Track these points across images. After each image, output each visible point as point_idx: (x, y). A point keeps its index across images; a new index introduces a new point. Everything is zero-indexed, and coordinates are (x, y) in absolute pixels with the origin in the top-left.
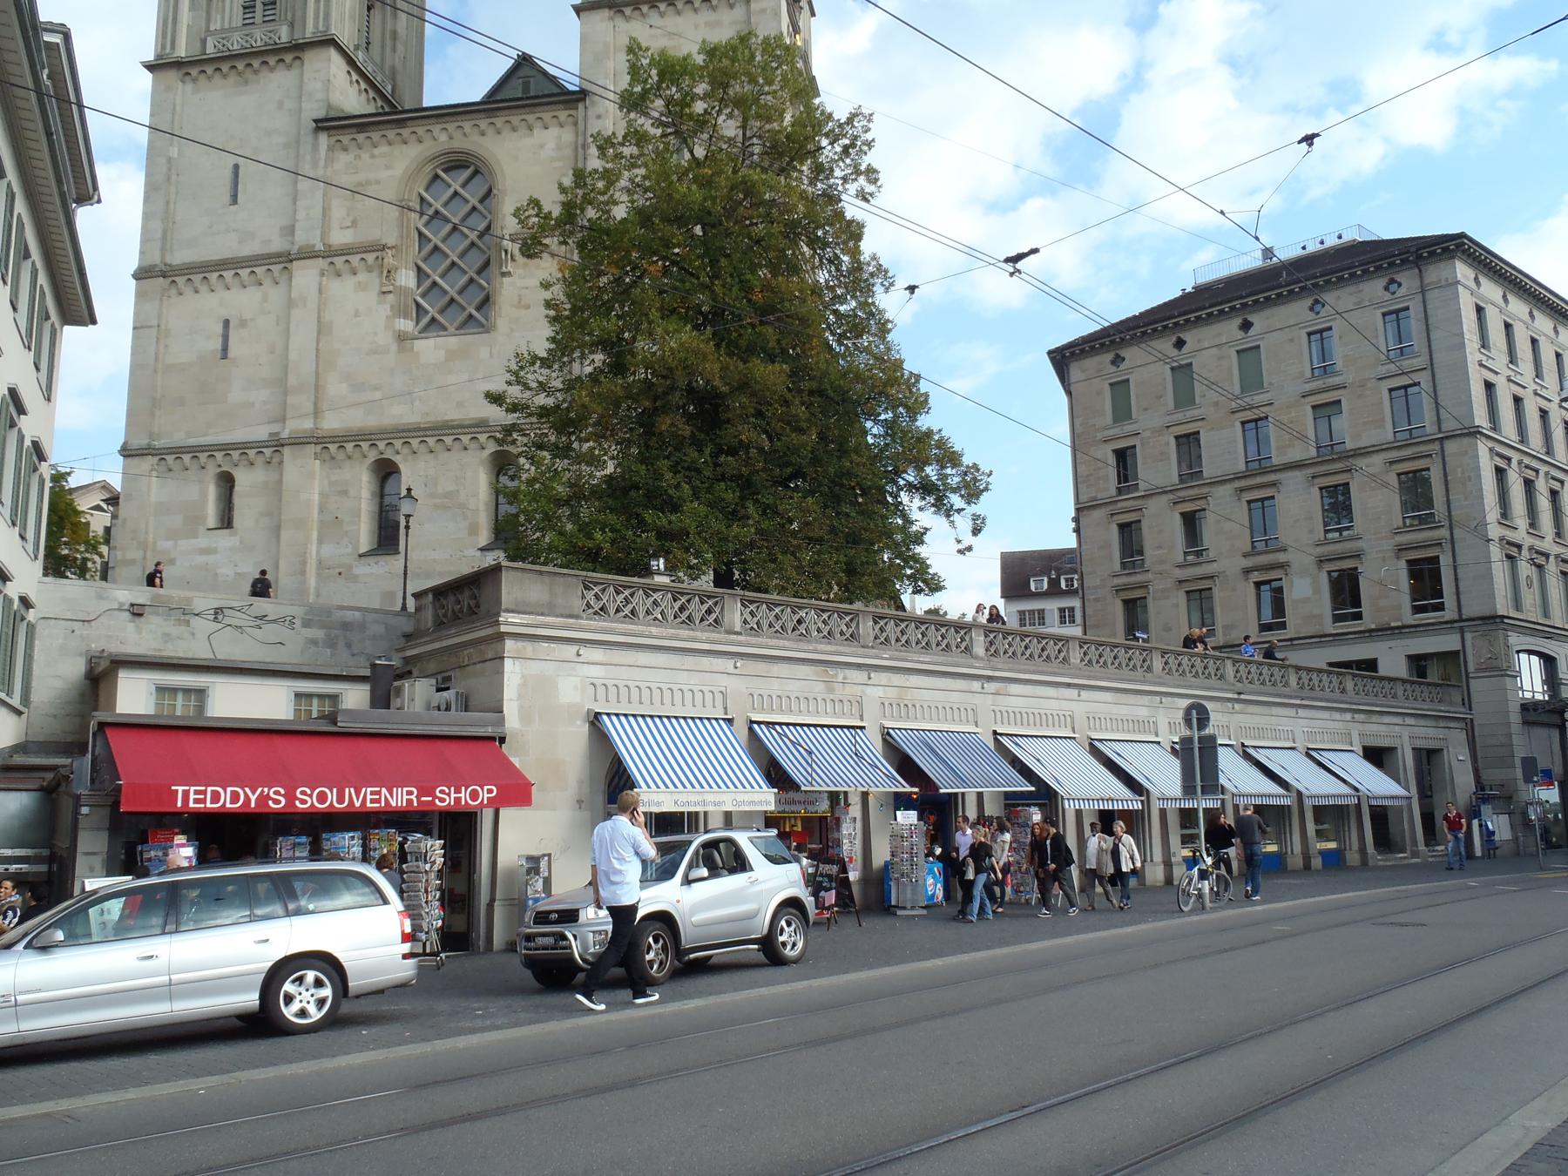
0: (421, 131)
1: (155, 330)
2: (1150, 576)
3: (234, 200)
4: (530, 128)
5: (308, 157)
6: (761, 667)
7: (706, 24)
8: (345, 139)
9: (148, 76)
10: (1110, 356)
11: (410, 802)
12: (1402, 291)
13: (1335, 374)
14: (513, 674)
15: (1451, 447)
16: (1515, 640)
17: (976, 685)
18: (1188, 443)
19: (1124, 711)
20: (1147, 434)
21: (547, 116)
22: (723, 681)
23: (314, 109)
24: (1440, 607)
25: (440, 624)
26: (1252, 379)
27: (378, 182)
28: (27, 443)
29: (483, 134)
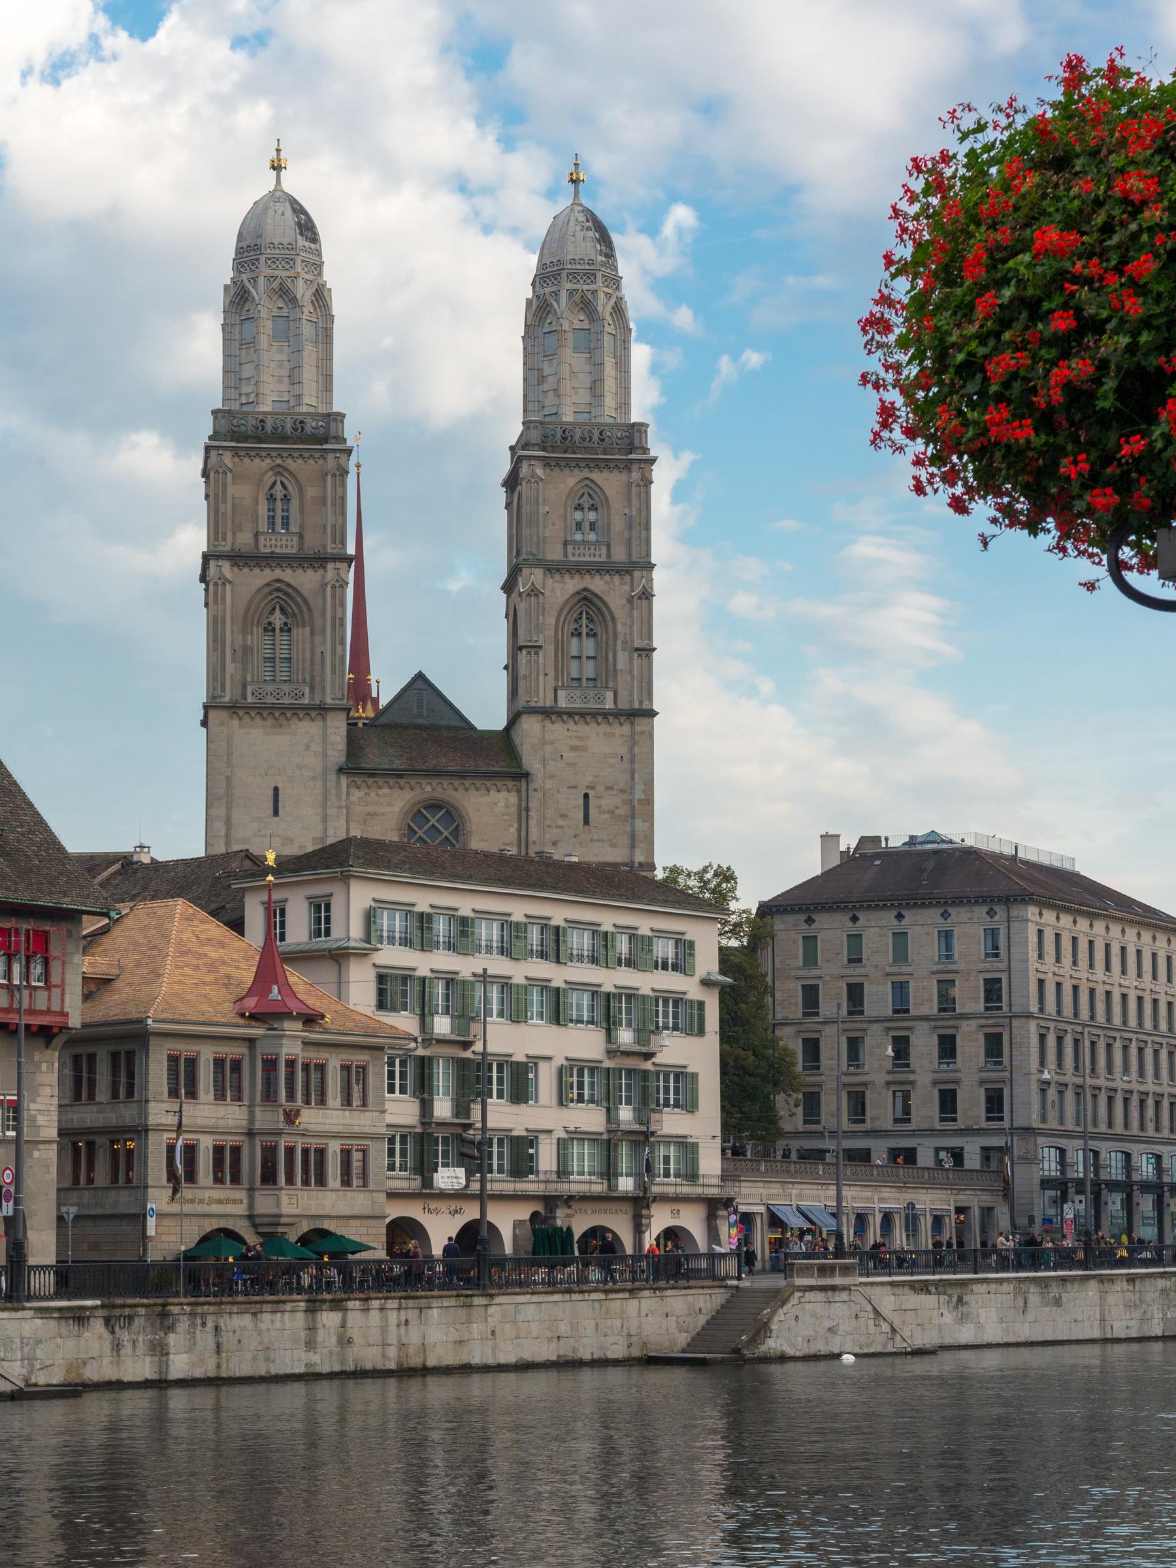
0: (413, 783)
2: (823, 1078)
3: (276, 813)
4: (488, 790)
5: (334, 791)
7: (605, 734)
8: (359, 781)
10: (804, 917)
12: (997, 918)
13: (954, 963)
15: (1016, 1023)
16: (1041, 1140)
18: (855, 993)
19: (864, 1194)
20: (828, 978)
21: (500, 784)
24: (1001, 1119)
26: (901, 953)
27: (383, 814)
29: (456, 790)
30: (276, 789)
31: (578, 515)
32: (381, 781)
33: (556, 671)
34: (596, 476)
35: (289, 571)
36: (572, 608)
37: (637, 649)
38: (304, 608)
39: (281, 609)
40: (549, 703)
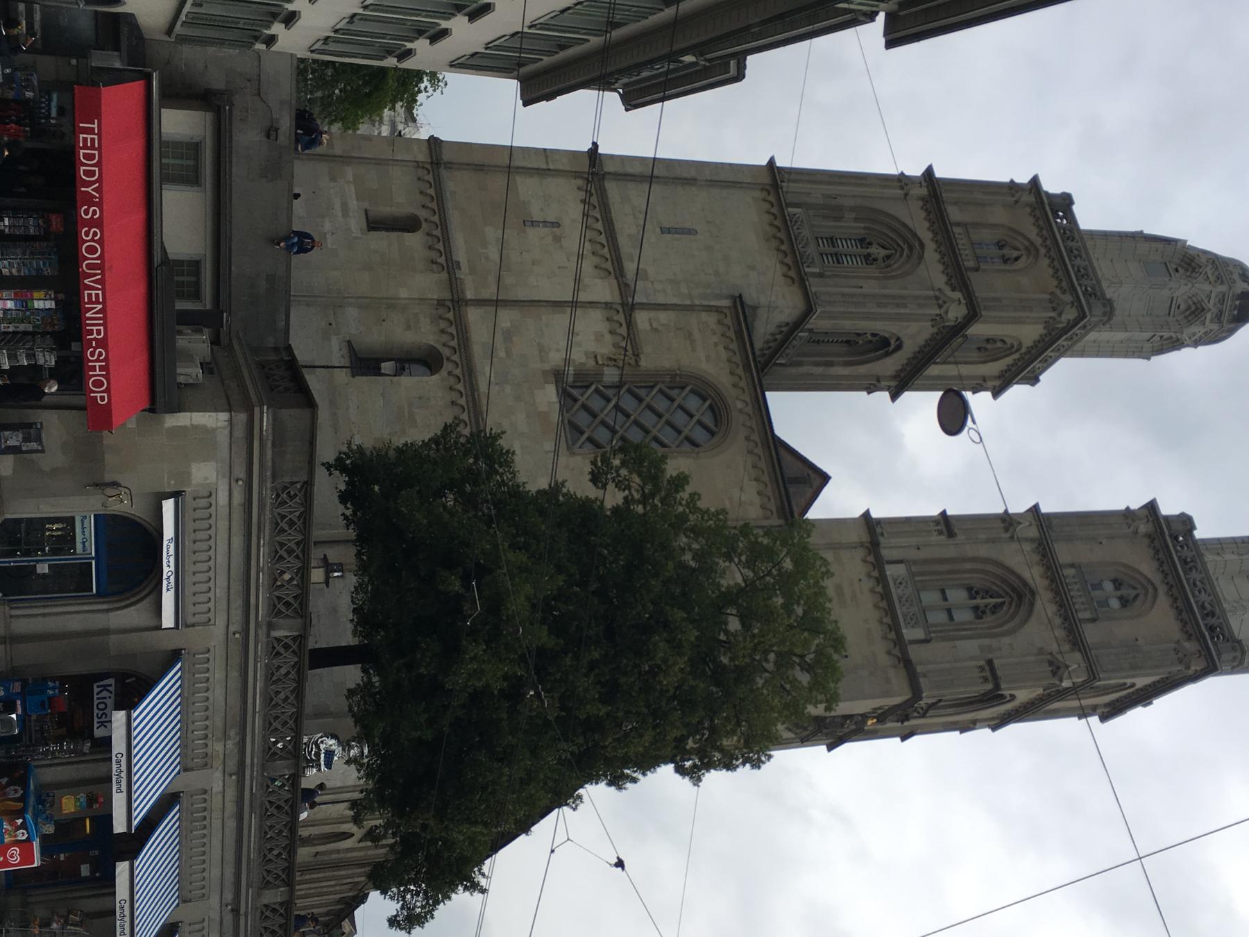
0: (743, 384)
1: (544, 166)
4: (757, 480)
6: (236, 660)
8: (728, 321)
9: (764, 162)
11: (91, 332)
14: (215, 420)
17: (229, 896)
21: (769, 491)
22: (220, 621)
23: (751, 297)
25: (262, 366)
27: (694, 350)
28: (409, 45)
30: (691, 232)
31: (1108, 586)
32: (734, 346)
33: (926, 562)
34: (1163, 601)
35: (937, 256)
36: (1004, 581)
37: (990, 662)
38: (899, 272)
39: (888, 257)
40: (886, 553)
